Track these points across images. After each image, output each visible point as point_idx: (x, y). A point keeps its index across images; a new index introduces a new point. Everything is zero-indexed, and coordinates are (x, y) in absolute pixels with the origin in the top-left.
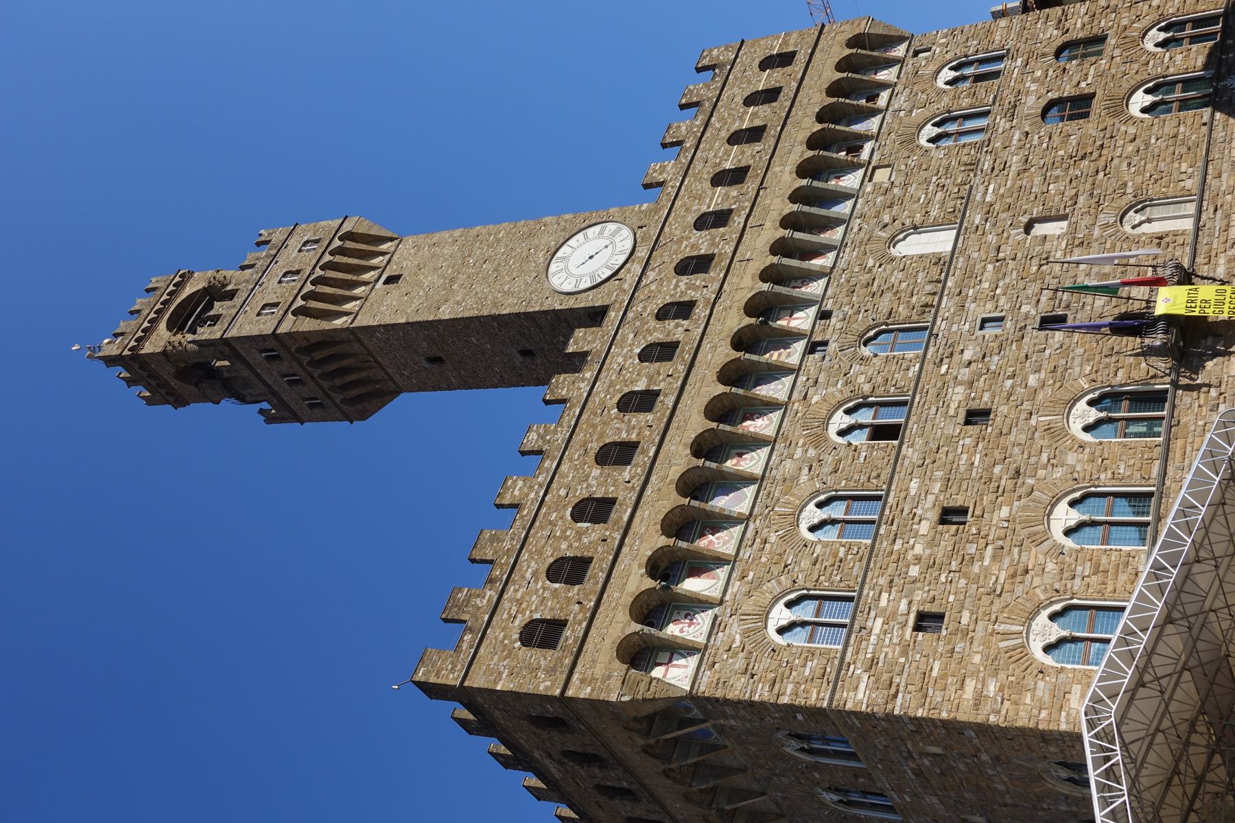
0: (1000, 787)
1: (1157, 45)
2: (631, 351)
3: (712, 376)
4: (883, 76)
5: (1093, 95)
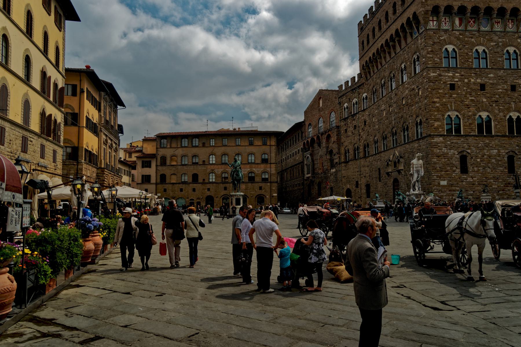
0: (413, 107)
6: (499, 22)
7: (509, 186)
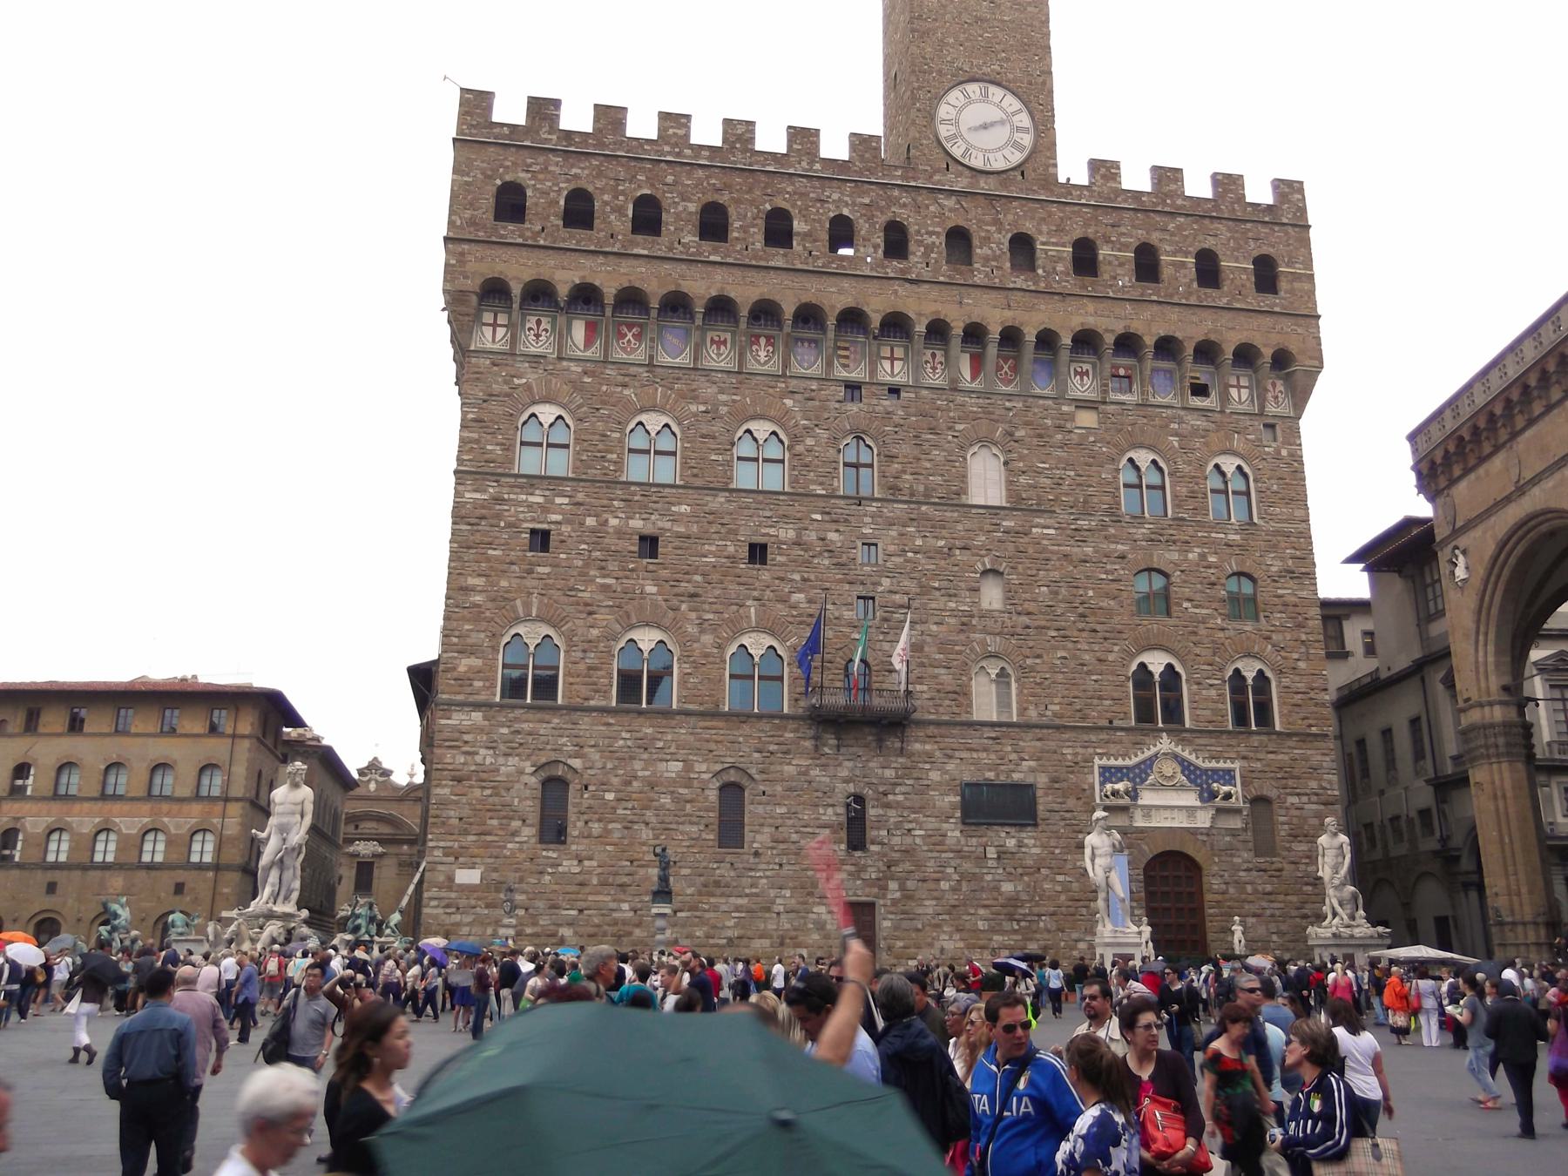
1: (1237, 671)
2: (847, 205)
3: (805, 299)
4: (1240, 396)
5: (1169, 614)
7: (718, 891)
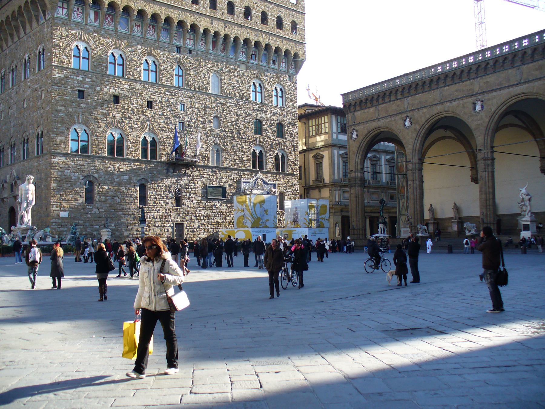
0: (35, 114)
4: (283, 65)
6: (139, 26)
